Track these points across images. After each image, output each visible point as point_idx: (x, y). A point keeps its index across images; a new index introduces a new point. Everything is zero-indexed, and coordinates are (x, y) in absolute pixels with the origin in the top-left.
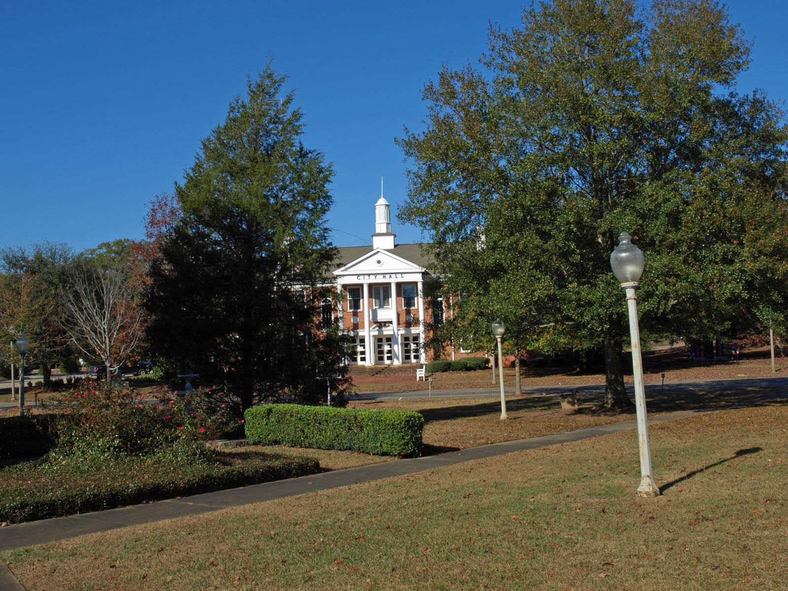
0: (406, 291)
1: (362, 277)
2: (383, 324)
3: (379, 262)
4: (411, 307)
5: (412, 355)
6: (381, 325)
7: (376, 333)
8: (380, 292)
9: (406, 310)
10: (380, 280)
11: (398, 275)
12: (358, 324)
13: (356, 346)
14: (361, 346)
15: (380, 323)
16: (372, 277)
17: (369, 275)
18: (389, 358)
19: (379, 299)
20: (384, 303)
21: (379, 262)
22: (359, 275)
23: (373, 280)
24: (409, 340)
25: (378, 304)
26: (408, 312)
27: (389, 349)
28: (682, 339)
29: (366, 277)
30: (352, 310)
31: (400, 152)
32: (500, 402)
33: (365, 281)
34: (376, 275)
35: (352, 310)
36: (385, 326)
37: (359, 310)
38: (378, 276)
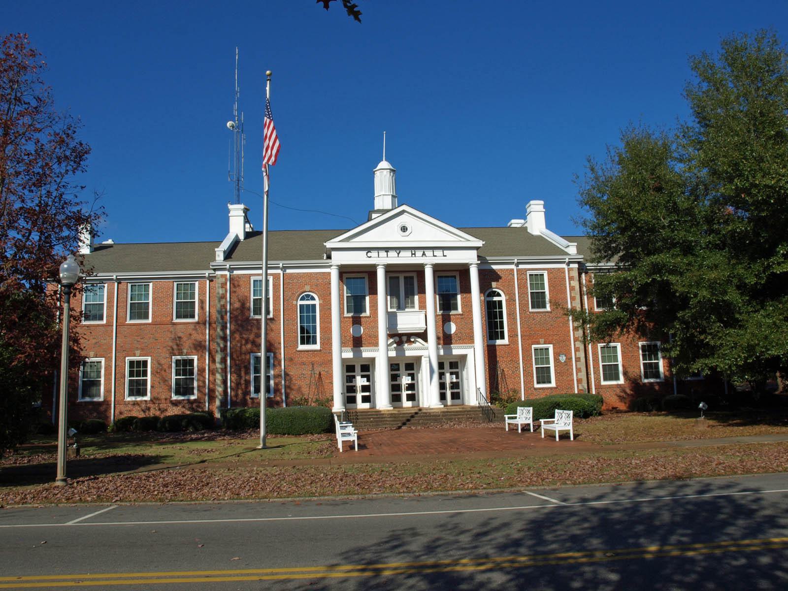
0: (451, 280)
1: (374, 254)
2: (404, 338)
3: (404, 229)
4: (450, 310)
5: (404, 394)
6: (400, 339)
7: (393, 354)
8: (405, 282)
9: (442, 315)
10: (406, 258)
11: (437, 253)
12: (361, 337)
13: (354, 377)
14: (363, 376)
15: (401, 335)
16: (392, 254)
17: (387, 250)
18: (366, 399)
19: (398, 298)
20: (406, 303)
21: (404, 229)
22: (369, 250)
23: (393, 259)
24: (398, 370)
25: (395, 305)
26: (357, 321)
27: (410, 382)
28: (651, 370)
29: (383, 254)
30: (350, 315)
31: (329, 9)
32: (56, 464)
33: (380, 260)
34: (399, 249)
35: (350, 315)
36: (409, 341)
37: (363, 315)
38: (403, 253)
